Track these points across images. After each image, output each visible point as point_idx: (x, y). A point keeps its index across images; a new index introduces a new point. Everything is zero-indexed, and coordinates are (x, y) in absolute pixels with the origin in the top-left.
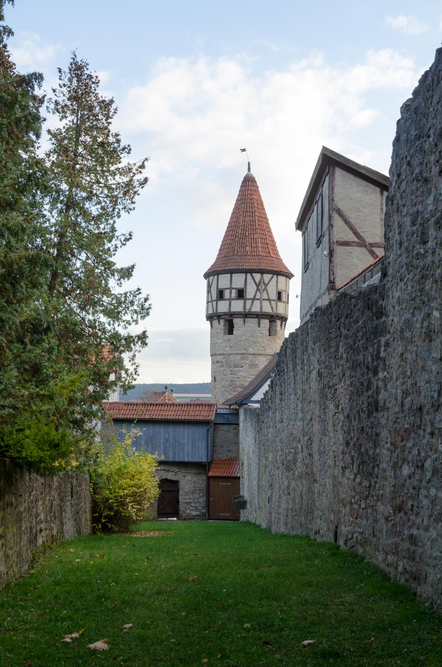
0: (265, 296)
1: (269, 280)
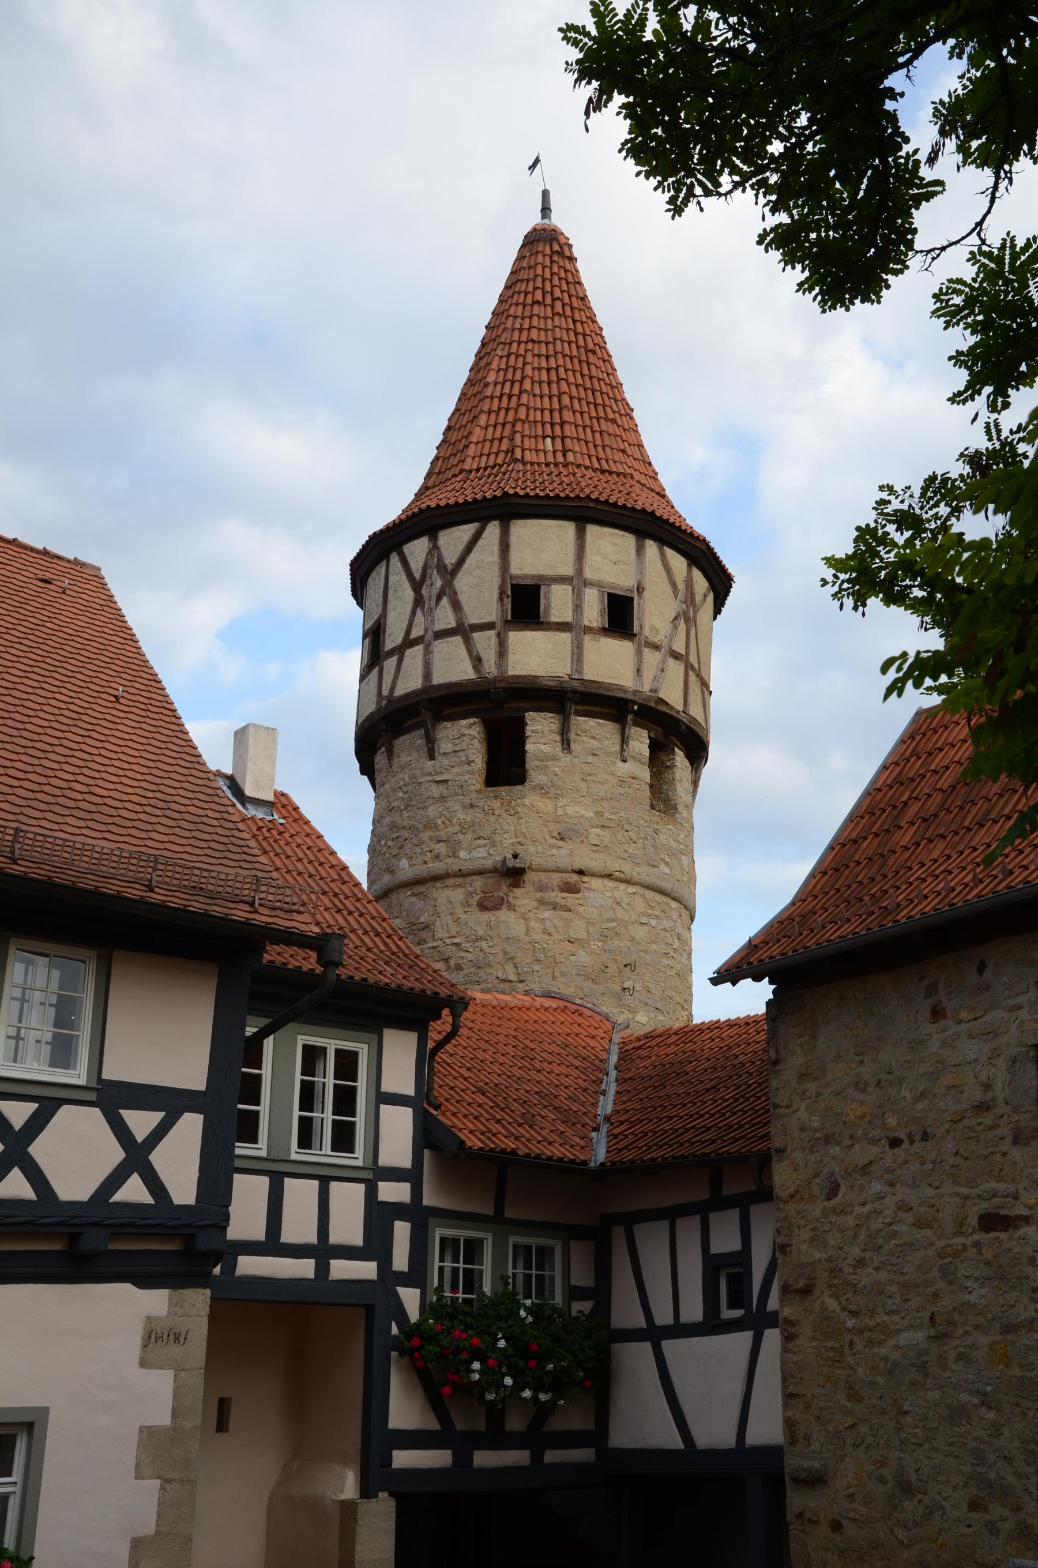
0: (445, 617)
1: (461, 548)
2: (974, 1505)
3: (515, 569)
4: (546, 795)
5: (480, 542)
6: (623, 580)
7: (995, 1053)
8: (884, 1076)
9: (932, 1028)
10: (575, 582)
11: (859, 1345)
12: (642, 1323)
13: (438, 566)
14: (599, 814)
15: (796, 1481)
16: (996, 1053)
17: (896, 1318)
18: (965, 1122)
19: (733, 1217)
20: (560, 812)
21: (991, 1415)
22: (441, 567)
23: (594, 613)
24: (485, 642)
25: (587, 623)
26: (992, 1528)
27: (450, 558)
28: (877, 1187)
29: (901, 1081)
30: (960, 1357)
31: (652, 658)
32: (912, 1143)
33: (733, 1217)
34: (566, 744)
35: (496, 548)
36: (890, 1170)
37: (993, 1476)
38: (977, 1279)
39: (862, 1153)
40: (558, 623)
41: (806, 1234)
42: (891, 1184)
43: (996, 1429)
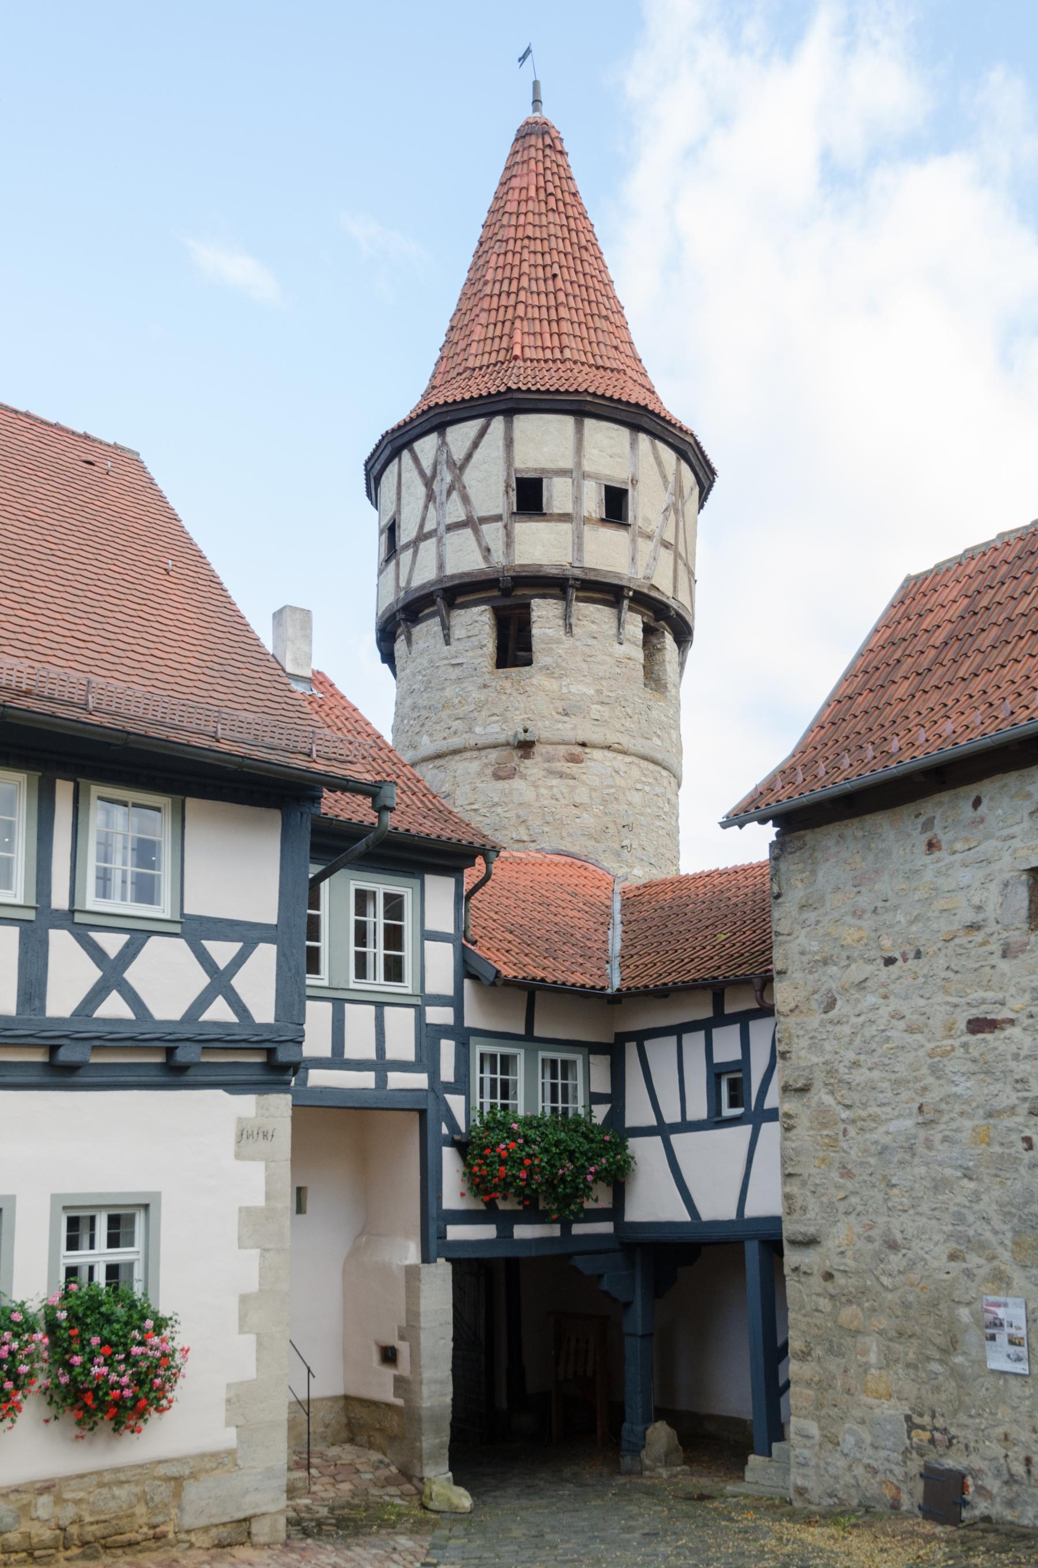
0: (455, 511)
1: (468, 444)
2: (953, 1257)
3: (518, 464)
4: (551, 675)
5: (486, 437)
6: (618, 476)
7: (989, 878)
8: (880, 904)
9: (928, 859)
10: (575, 474)
11: (852, 1131)
12: (653, 1121)
13: (447, 462)
14: (599, 692)
15: (793, 1243)
16: (989, 878)
17: (887, 1109)
18: (957, 941)
19: (735, 1029)
20: (564, 690)
21: (972, 1185)
22: (451, 463)
23: (593, 504)
24: (493, 533)
25: (586, 514)
26: (969, 1274)
27: (458, 455)
28: (871, 999)
29: (896, 908)
30: (945, 1139)
31: (646, 547)
32: (905, 960)
33: (733, 1031)
34: (569, 628)
35: (501, 443)
36: (884, 985)
37: (971, 1233)
38: (963, 1074)
39: (857, 971)
40: (560, 515)
41: (805, 1042)
42: (885, 997)
43: (976, 1197)
